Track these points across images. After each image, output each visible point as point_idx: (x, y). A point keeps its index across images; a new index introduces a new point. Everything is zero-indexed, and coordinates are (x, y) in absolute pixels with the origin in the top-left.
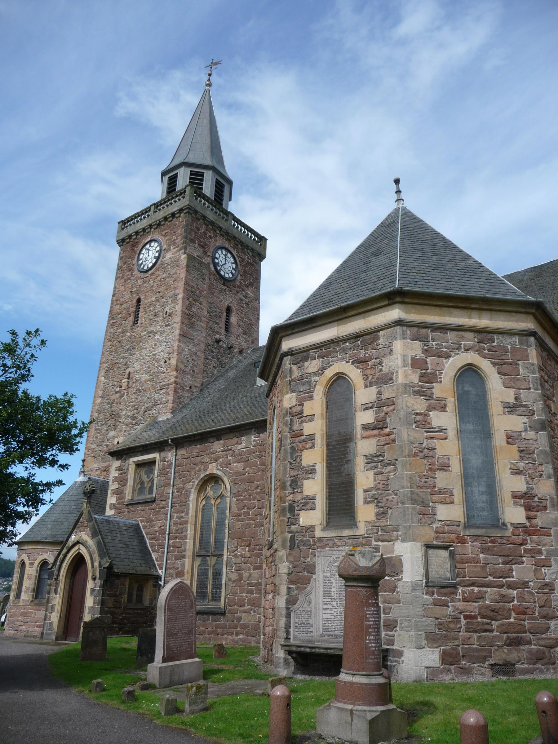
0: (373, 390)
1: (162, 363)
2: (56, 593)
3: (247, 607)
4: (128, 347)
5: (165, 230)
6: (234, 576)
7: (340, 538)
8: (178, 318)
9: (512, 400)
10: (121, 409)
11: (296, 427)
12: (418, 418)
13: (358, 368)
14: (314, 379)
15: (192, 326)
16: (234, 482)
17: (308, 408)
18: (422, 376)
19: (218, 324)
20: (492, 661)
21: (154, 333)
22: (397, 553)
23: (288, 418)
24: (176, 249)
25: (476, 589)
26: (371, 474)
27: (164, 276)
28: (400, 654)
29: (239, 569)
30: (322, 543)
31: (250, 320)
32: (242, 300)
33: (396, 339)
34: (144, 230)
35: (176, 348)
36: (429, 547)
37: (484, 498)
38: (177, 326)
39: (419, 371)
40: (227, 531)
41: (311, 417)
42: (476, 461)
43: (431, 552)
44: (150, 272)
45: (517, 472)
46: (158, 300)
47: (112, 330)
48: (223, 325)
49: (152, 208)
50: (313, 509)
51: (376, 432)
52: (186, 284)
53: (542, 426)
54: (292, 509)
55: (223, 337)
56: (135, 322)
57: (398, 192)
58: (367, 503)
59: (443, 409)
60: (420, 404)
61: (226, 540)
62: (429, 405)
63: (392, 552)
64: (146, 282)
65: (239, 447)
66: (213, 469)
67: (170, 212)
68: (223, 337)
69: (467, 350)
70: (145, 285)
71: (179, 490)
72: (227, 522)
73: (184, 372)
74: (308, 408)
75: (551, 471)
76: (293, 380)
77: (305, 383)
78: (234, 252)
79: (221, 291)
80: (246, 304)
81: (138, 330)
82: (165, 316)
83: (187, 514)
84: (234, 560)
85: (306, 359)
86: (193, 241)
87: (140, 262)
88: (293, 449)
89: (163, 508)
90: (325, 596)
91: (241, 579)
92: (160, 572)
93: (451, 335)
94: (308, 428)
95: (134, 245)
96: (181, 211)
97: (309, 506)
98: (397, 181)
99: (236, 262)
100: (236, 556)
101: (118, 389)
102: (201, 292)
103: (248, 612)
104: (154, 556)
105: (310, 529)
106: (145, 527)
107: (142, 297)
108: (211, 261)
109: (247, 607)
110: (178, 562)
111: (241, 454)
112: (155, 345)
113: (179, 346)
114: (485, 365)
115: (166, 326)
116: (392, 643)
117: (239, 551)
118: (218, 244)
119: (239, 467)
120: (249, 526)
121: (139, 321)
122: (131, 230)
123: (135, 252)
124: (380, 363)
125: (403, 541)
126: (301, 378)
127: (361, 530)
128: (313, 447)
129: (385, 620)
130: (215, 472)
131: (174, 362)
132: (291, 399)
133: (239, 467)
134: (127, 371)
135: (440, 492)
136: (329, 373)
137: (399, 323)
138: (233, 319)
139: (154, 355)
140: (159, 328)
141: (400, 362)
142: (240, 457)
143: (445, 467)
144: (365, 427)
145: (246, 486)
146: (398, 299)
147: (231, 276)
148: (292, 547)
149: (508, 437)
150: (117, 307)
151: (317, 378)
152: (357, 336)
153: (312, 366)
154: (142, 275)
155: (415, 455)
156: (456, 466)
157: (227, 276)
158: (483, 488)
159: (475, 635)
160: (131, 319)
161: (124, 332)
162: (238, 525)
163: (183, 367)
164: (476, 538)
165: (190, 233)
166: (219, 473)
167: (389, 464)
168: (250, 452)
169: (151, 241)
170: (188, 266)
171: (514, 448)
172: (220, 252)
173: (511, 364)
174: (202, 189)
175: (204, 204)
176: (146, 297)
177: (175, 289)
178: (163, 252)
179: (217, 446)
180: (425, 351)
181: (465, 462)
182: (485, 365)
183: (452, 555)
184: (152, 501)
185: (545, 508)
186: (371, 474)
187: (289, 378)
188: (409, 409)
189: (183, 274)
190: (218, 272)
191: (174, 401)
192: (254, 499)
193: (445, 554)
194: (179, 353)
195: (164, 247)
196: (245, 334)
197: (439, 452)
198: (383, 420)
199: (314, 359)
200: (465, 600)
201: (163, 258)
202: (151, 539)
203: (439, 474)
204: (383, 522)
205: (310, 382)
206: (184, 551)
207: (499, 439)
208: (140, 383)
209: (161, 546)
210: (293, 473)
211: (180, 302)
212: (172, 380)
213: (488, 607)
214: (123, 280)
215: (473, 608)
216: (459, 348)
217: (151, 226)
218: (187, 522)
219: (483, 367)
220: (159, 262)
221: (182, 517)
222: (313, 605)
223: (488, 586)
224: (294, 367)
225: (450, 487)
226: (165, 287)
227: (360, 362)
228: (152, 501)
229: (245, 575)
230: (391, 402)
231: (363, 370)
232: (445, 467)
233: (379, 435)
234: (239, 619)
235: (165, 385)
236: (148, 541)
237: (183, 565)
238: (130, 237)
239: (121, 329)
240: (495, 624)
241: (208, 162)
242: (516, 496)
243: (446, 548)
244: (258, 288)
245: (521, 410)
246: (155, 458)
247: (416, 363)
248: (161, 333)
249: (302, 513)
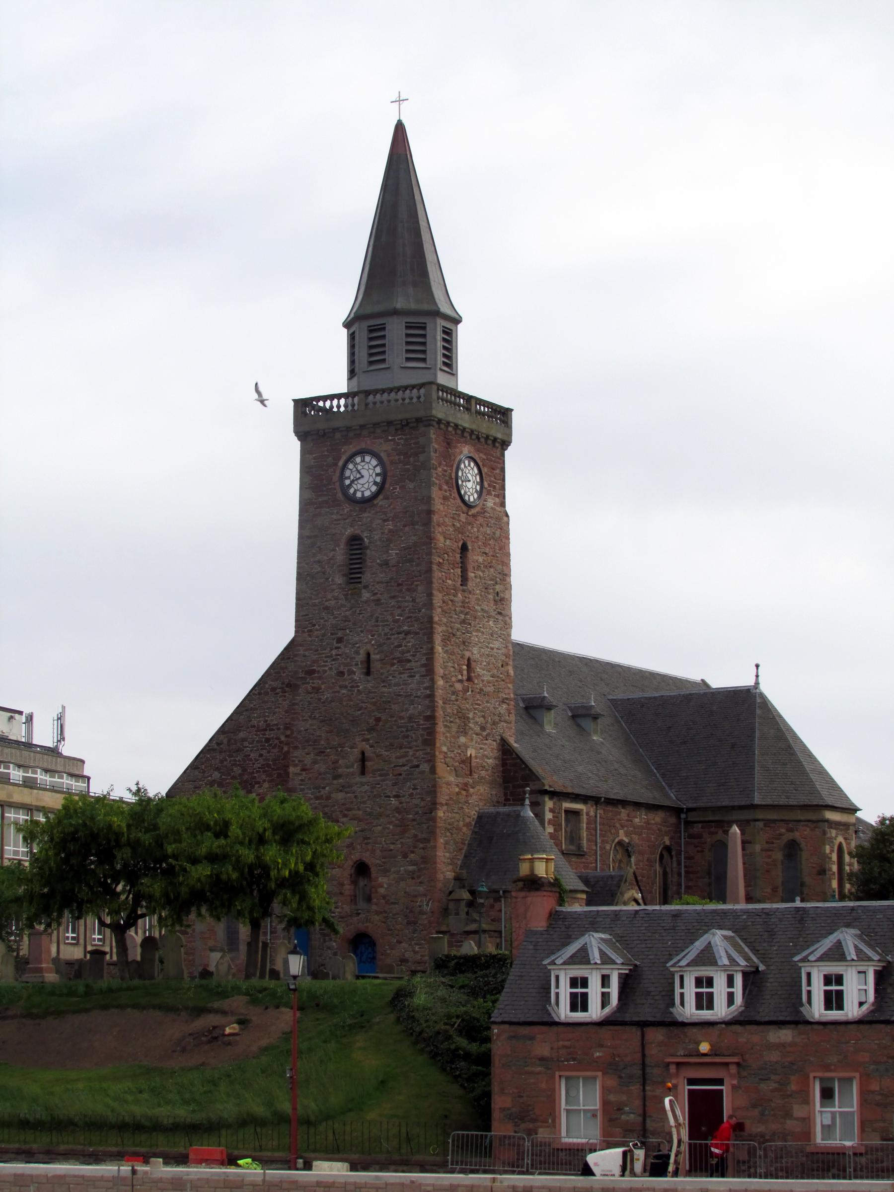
1: (500, 665)
4: (463, 616)
10: (467, 709)
21: (489, 617)
47: (440, 574)
56: (464, 579)
57: (757, 676)
64: (470, 524)
70: (470, 528)
82: (497, 598)
98: (757, 666)
112: (492, 635)
115: (500, 613)
154: (464, 508)
160: (459, 571)
169: (471, 458)
195: (486, 484)
208: (483, 681)
235: (507, 699)
238: (448, 423)
239: (450, 582)
246: (582, 810)
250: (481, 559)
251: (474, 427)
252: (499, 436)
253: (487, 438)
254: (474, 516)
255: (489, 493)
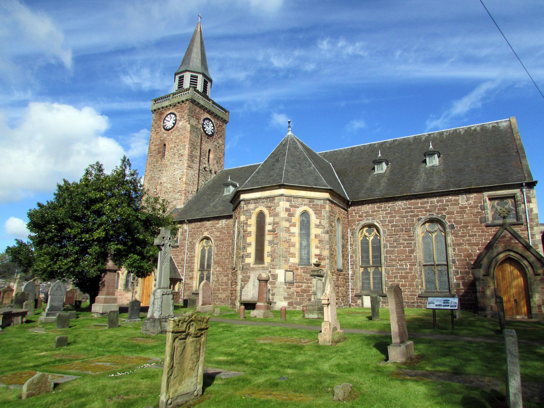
0: (272, 218)
1: (178, 179)
2: (137, 286)
3: (221, 291)
5: (178, 109)
6: (216, 279)
7: (259, 268)
8: (186, 158)
9: (318, 223)
11: (245, 228)
12: (286, 229)
13: (267, 209)
14: (252, 211)
15: (193, 161)
16: (216, 240)
17: (249, 222)
18: (289, 214)
19: (204, 159)
20: (303, 305)
21: (174, 164)
22: (276, 273)
23: (242, 225)
24: (185, 121)
25: (300, 284)
26: (270, 247)
27: (178, 134)
28: (275, 303)
29: (217, 276)
30: (253, 269)
31: (220, 156)
32: (216, 145)
33: (281, 201)
34: (167, 107)
35: (185, 173)
36: (286, 271)
37: (306, 255)
38: (186, 162)
39: (288, 213)
40: (212, 261)
41: (250, 225)
42: (305, 243)
43: (287, 272)
44: (170, 131)
45: (317, 247)
46: (175, 147)
48: (207, 159)
49: (171, 95)
50: (250, 257)
51: (272, 233)
52: (190, 140)
53: (327, 232)
54: (243, 257)
55: (207, 166)
58: (268, 256)
59: (295, 226)
60: (287, 224)
61: (212, 265)
62: (290, 225)
63: (275, 272)
65: (218, 225)
66: (206, 234)
67: (181, 100)
68: (207, 166)
69: (305, 205)
71: (190, 242)
72: (212, 257)
73: (189, 184)
74: (249, 222)
75: (328, 247)
76: (244, 211)
77: (249, 212)
78: (213, 121)
79: (206, 142)
80: (218, 147)
81: (165, 161)
83: (194, 253)
84: (215, 272)
85: (249, 203)
86: (193, 117)
87: (165, 124)
88: (244, 236)
89: (183, 250)
90: (253, 286)
91: (218, 280)
92: (182, 277)
93: (300, 200)
94: (249, 229)
95: (161, 114)
96: (187, 100)
97: (249, 256)
99: (214, 126)
100: (216, 271)
101: (155, 190)
102: (197, 143)
103: (222, 293)
104: (179, 270)
105: (249, 264)
106: (174, 258)
107: (167, 144)
108: (201, 127)
109: (221, 291)
110: (190, 273)
111: (218, 228)
112: (175, 170)
113: (187, 172)
114: (311, 211)
115: (180, 161)
116: (273, 300)
117: (218, 269)
118: (205, 117)
119: (218, 234)
120: (222, 259)
121: (165, 156)
122: (159, 105)
123: (162, 118)
124: (275, 209)
125: (279, 269)
126: (247, 211)
127: (266, 265)
128: (251, 236)
129: (272, 293)
130: (207, 235)
131: (184, 180)
132: (243, 218)
133: (218, 234)
134: (160, 181)
135: (291, 254)
136: (258, 210)
137: (282, 195)
138: (211, 156)
139: (174, 175)
140: (176, 161)
141: (282, 210)
142: (218, 230)
143: (294, 246)
144: (269, 231)
145: (221, 243)
146: (282, 187)
147: (211, 133)
148: (242, 270)
149: (315, 236)
150: (153, 147)
151: (253, 211)
152: (268, 198)
153: (251, 206)
154: (166, 132)
155: (284, 241)
156: (297, 245)
157: (209, 133)
158: (306, 252)
159: (299, 298)
161: (157, 161)
162: (218, 258)
163: (189, 182)
164: (302, 268)
165: (192, 113)
166: (209, 236)
167: (276, 244)
168: (223, 228)
170: (191, 131)
171: (317, 240)
172: (206, 121)
173: (319, 210)
174: (196, 87)
175: (199, 96)
176: (169, 144)
177: (184, 142)
178: (177, 121)
179: (208, 224)
180: (290, 206)
181: (301, 244)
182: (311, 211)
183: (293, 273)
184: (178, 247)
185: (325, 259)
186: (270, 247)
187: (243, 210)
188: (284, 226)
189: (188, 135)
190: (205, 132)
191: (185, 199)
192: (224, 248)
193: (292, 273)
194: (187, 176)
195: (178, 118)
196: (217, 163)
197: (292, 241)
198: (275, 229)
199: (252, 203)
200: (296, 287)
201: (178, 124)
202: (177, 263)
203: (292, 248)
204: (273, 263)
205: (250, 212)
206: (193, 268)
207: (312, 237)
209: (183, 266)
210: (243, 245)
211: (187, 149)
212: (184, 189)
213: (303, 289)
214: (155, 133)
215: (299, 290)
216: (302, 205)
217: (170, 105)
218: (194, 256)
219: (309, 211)
220: (175, 126)
221: (192, 254)
222: (249, 289)
223: (304, 283)
224: (245, 206)
225: (295, 252)
226: (179, 140)
227: (269, 208)
228: (178, 247)
229: (220, 279)
230: (277, 223)
231: (269, 210)
232: (294, 246)
233: (273, 234)
234: (217, 296)
236: (176, 264)
237: (193, 274)
238: (159, 109)
240: (305, 294)
241: (200, 71)
242: (316, 255)
243: (292, 271)
244: (224, 138)
245: (321, 226)
247: (287, 210)
248: (178, 164)
249: (246, 259)
250: (173, 146)
251: (170, 104)
252: (184, 99)
253: (179, 103)
254: (171, 132)
255: (180, 120)
